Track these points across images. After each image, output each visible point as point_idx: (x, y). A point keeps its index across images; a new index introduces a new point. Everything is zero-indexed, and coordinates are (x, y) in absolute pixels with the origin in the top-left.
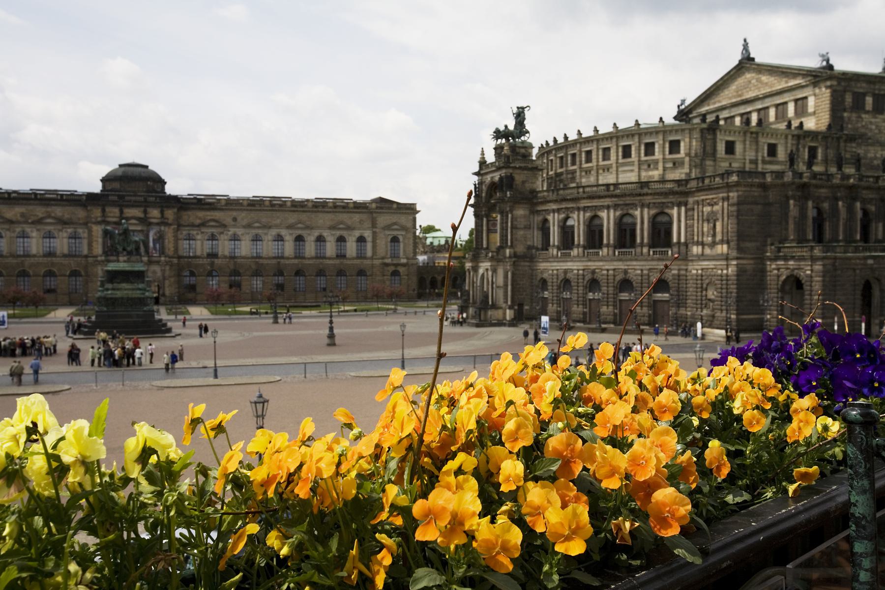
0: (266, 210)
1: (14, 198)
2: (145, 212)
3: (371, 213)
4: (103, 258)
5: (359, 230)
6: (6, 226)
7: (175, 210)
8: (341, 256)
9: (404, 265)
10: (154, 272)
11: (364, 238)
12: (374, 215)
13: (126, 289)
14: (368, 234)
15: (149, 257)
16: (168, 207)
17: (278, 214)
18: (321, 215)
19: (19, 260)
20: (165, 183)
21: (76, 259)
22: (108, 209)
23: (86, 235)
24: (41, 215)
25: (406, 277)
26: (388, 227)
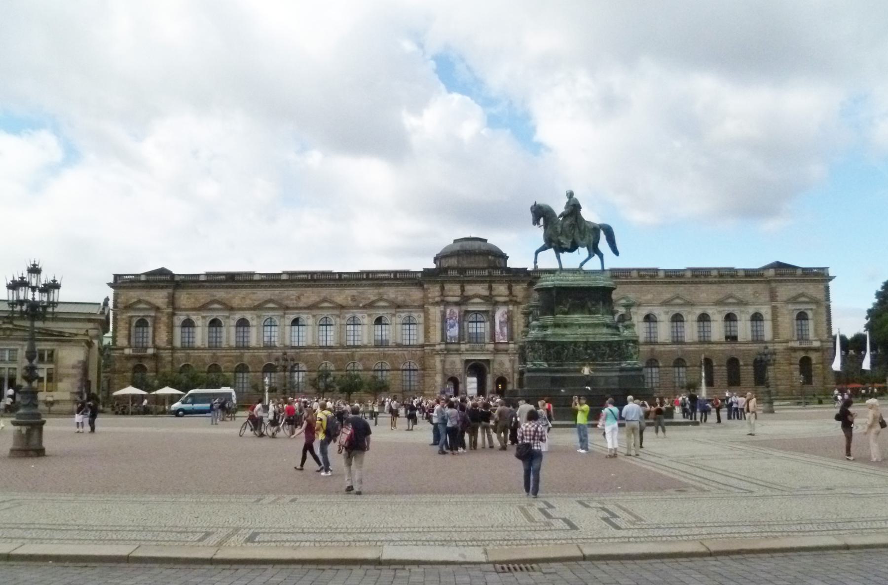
0: (635, 283)
1: (345, 279)
2: (490, 289)
3: (769, 282)
4: (443, 346)
5: (754, 305)
6: (337, 312)
7: (525, 285)
8: (732, 338)
9: (816, 350)
10: (501, 364)
11: (761, 315)
12: (774, 285)
13: (580, 326)
14: (765, 311)
15: (495, 343)
16: (517, 282)
17: (650, 287)
18: (704, 287)
19: (349, 352)
20: (508, 257)
21: (410, 349)
22: (447, 287)
23: (421, 320)
24: (373, 298)
25: (821, 366)
26: (794, 300)
